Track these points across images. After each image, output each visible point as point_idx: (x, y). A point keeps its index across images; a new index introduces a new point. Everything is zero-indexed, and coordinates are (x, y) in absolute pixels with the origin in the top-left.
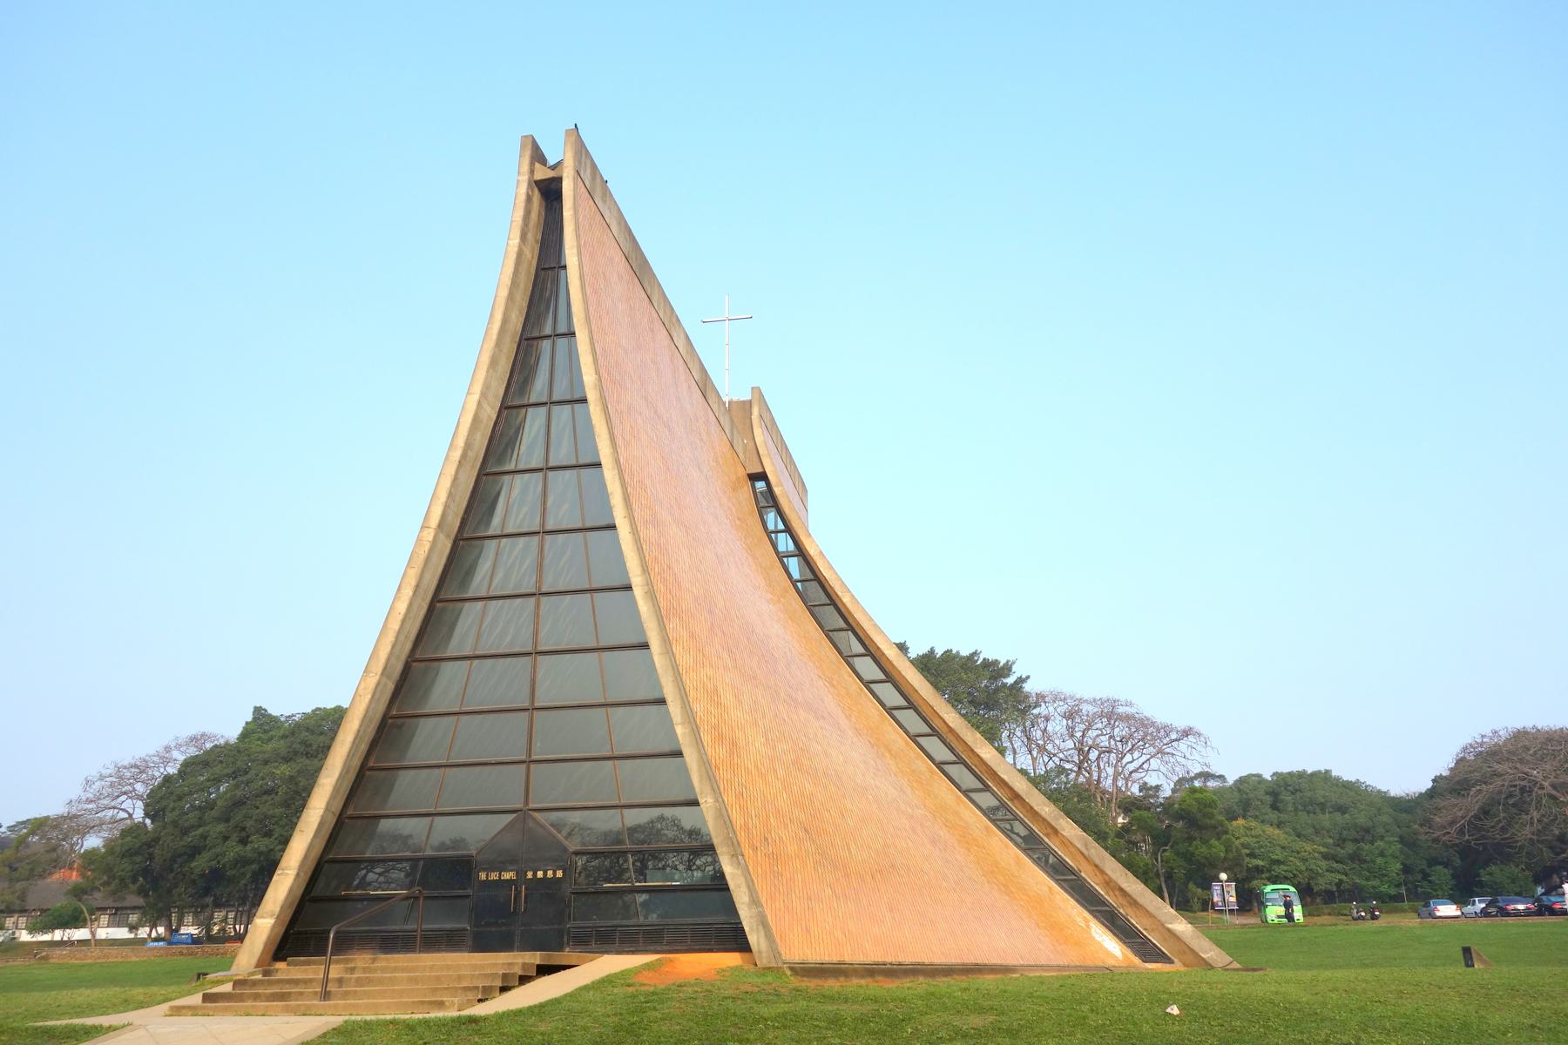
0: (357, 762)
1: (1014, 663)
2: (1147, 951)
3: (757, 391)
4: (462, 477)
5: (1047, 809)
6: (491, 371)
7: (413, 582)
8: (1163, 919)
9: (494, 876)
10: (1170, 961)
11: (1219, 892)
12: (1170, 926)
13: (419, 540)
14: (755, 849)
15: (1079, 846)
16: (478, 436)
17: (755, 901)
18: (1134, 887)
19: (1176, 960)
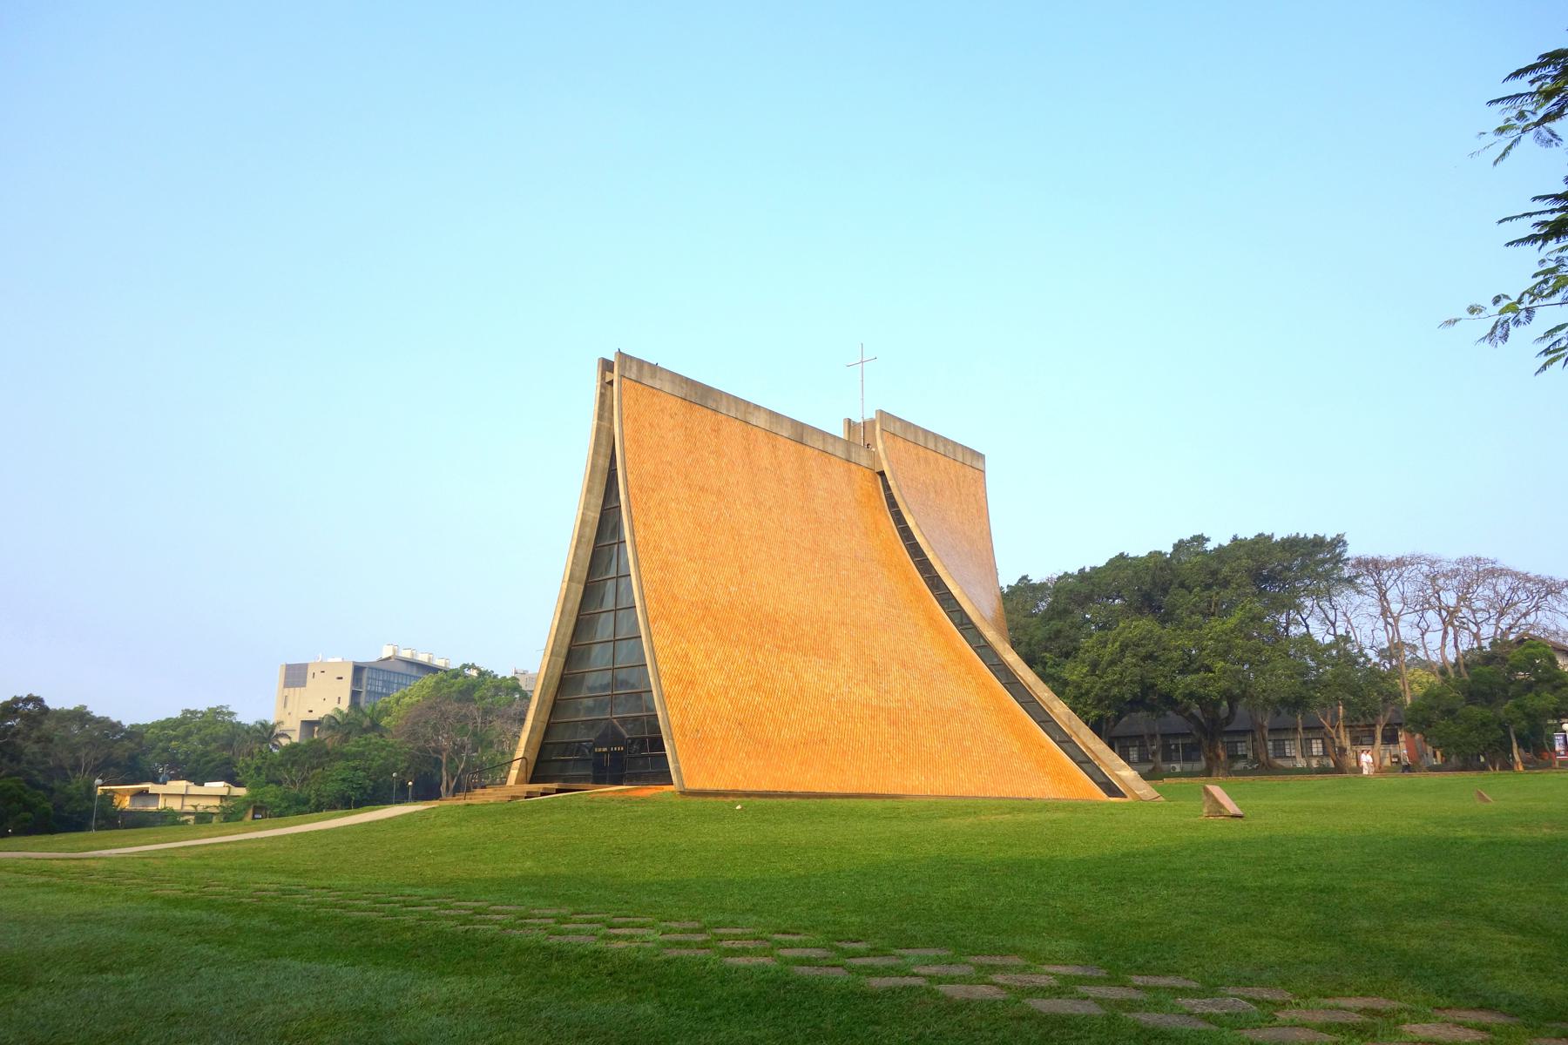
0: (550, 698)
1: (1343, 536)
2: (1110, 789)
3: (881, 413)
4: (580, 552)
5: (1046, 695)
6: (588, 496)
7: (560, 610)
8: (1113, 768)
9: (600, 750)
10: (1125, 797)
11: (1562, 742)
12: (1118, 773)
13: (561, 589)
14: (684, 735)
15: (1064, 720)
16: (588, 530)
17: (676, 761)
18: (1098, 746)
19: (1128, 796)
